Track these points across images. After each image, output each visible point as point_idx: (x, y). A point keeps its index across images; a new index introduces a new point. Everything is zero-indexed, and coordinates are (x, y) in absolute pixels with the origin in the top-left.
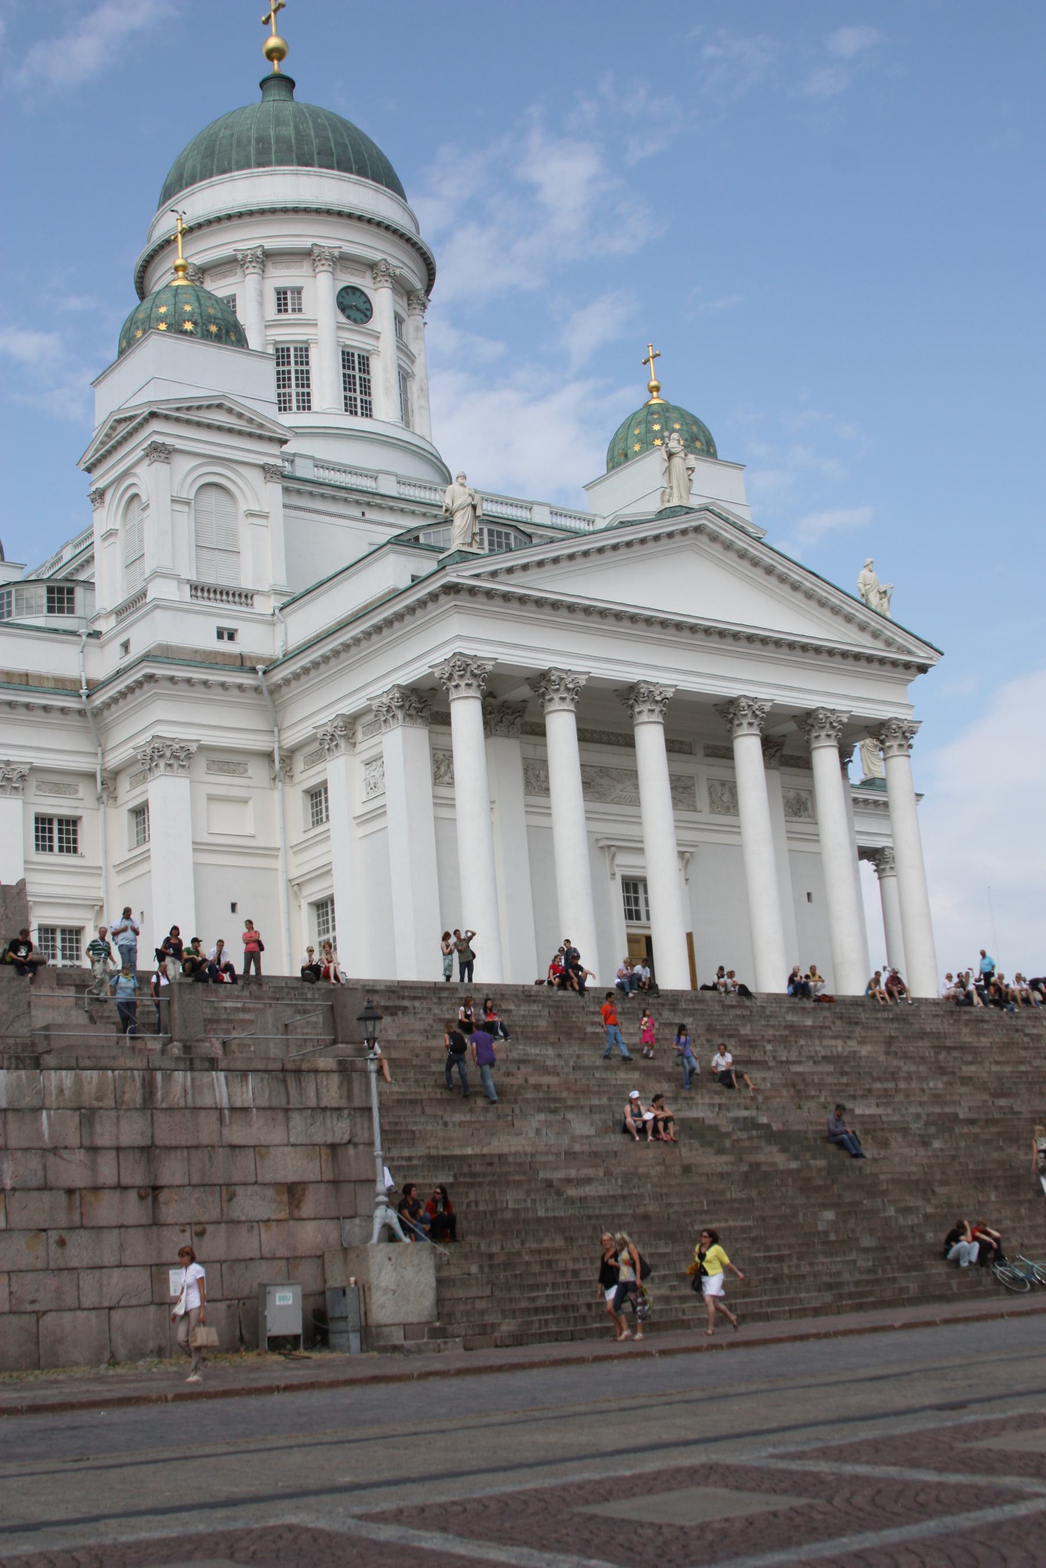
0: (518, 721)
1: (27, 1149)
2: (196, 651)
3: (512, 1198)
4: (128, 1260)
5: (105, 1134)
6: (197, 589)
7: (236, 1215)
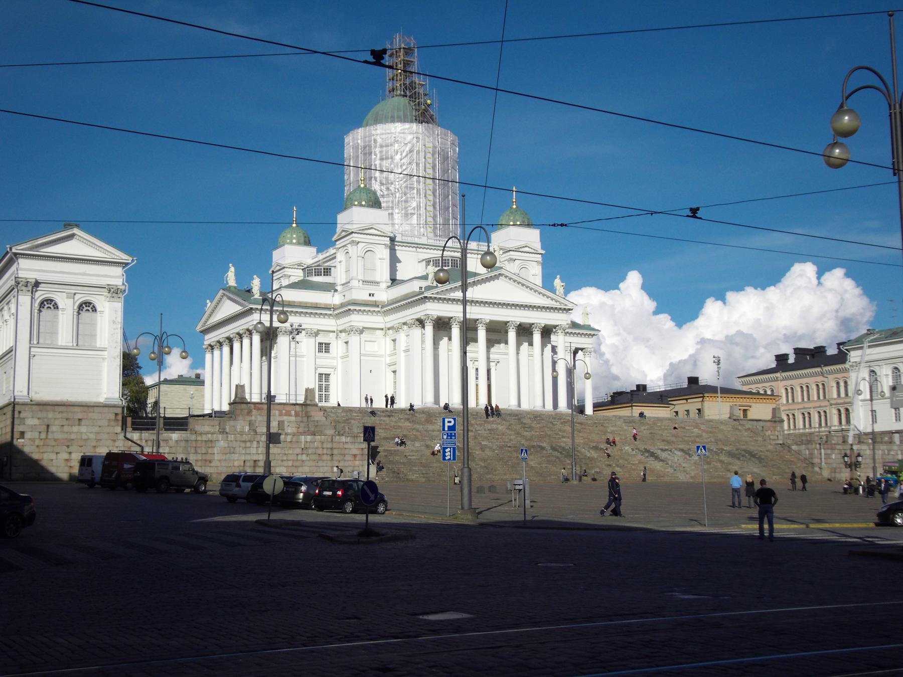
0: (448, 326)
1: (313, 448)
2: (363, 301)
3: (397, 458)
4: (328, 465)
5: (325, 446)
6: (365, 282)
7: (345, 458)
